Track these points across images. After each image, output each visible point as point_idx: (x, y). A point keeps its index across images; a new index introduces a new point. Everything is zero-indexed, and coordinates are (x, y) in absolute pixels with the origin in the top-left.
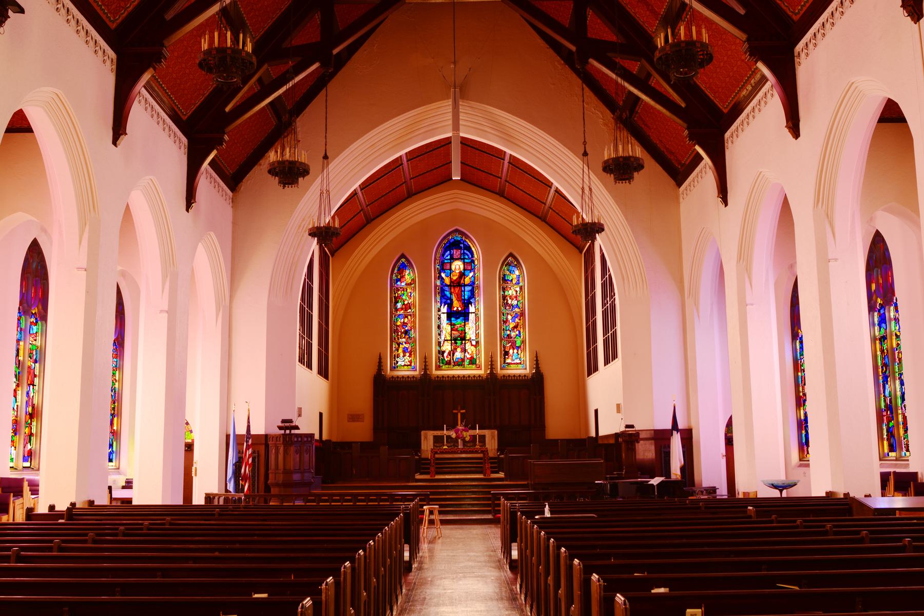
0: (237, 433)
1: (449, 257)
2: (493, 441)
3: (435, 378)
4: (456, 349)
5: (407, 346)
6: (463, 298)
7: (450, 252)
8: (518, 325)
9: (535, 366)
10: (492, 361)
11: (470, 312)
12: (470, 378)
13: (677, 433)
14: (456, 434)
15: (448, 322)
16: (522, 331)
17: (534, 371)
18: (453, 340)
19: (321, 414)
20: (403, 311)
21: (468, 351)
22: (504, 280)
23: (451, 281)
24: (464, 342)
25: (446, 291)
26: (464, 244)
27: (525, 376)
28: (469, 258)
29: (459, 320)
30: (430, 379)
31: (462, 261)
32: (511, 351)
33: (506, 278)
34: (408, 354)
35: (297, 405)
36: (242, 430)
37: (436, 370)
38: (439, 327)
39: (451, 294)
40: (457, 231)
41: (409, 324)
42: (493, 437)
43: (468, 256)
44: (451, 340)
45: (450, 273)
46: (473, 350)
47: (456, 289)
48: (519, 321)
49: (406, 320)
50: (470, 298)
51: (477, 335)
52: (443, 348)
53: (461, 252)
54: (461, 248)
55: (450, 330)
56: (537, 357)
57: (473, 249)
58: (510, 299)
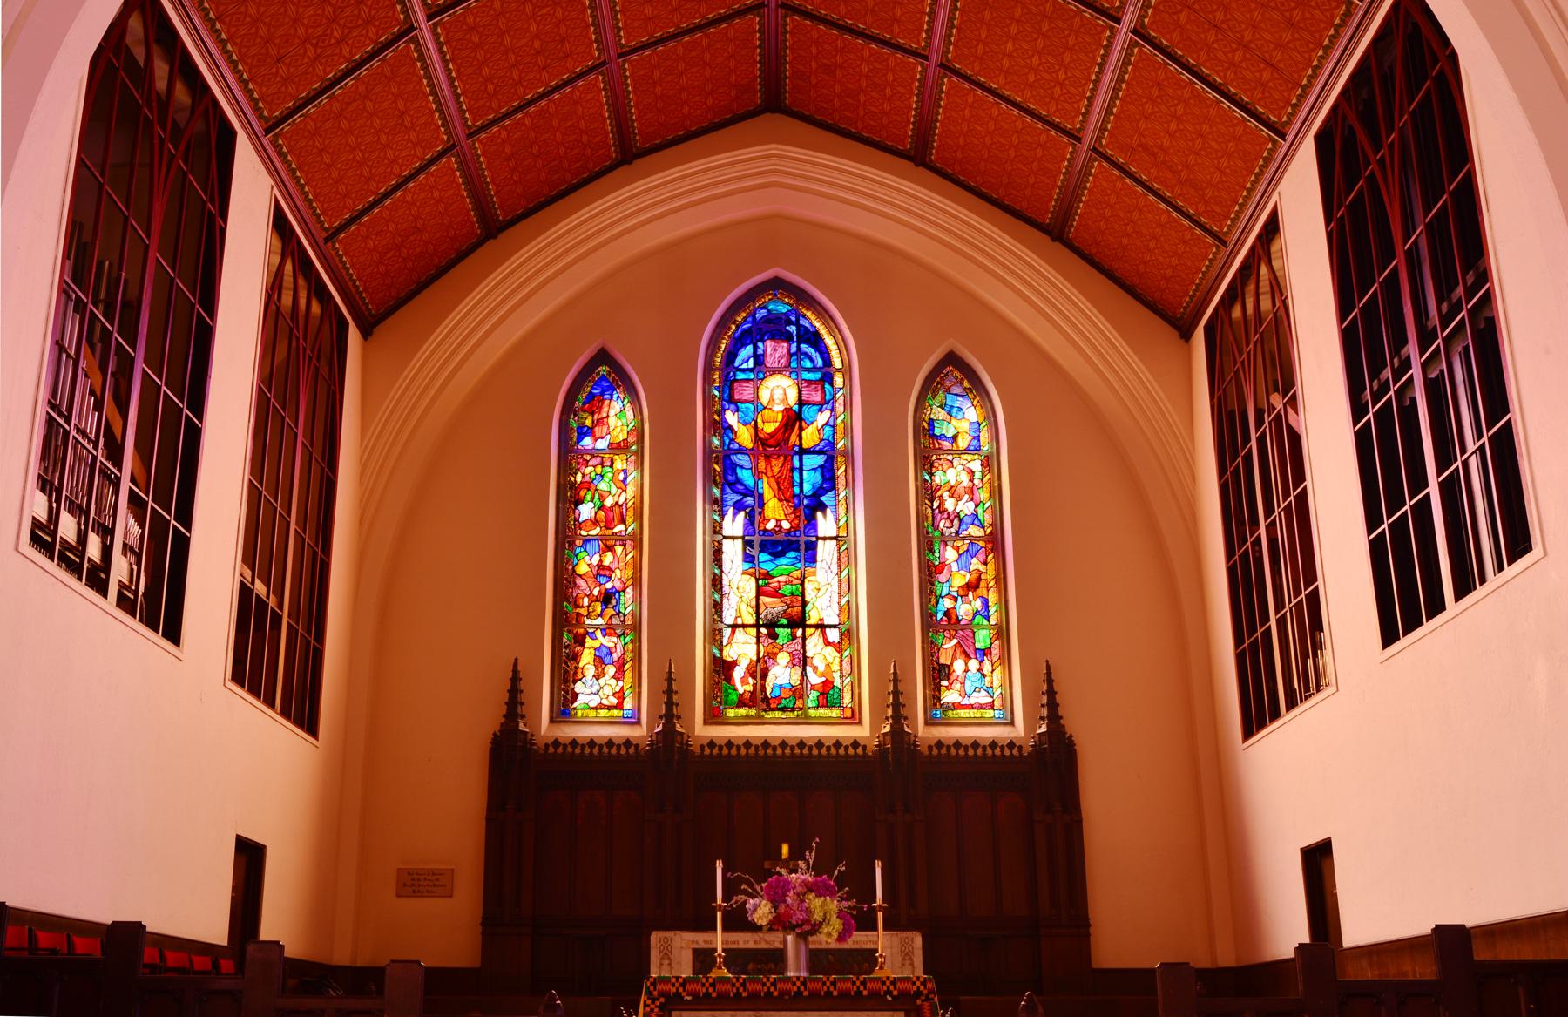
1: (751, 364)
3: (702, 747)
4: (772, 656)
5: (609, 642)
6: (797, 490)
7: (756, 348)
8: (979, 579)
9: (1045, 712)
10: (896, 693)
11: (820, 534)
12: (824, 751)
15: (747, 566)
16: (992, 598)
18: (763, 626)
20: (598, 529)
21: (815, 662)
22: (926, 433)
23: (757, 435)
24: (799, 632)
25: (742, 467)
26: (797, 324)
28: (814, 369)
29: (783, 561)
31: (794, 376)
32: (959, 666)
33: (937, 432)
34: (611, 670)
37: (705, 723)
38: (716, 583)
39: (758, 475)
40: (777, 286)
41: (618, 571)
43: (812, 360)
44: (757, 626)
45: (756, 411)
46: (830, 660)
47: (774, 462)
48: (982, 568)
49: (608, 559)
50: (819, 492)
51: (847, 610)
52: (729, 654)
53: (789, 349)
54: (788, 338)
55: (753, 593)
56: (1050, 681)
57: (829, 341)
58: (951, 496)
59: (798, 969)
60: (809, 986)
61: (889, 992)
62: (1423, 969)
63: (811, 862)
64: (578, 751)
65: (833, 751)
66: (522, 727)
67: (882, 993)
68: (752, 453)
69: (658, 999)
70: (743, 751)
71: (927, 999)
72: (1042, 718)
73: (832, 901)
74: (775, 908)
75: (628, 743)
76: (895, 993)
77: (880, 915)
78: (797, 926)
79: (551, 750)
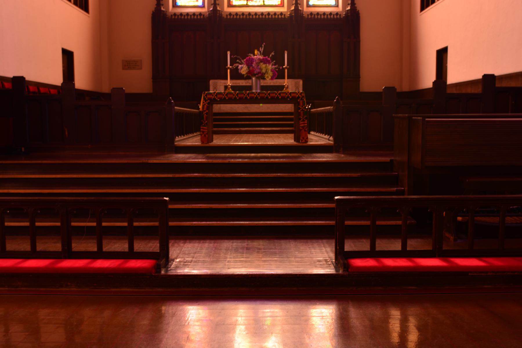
3: (227, 15)
27: (337, 14)
30: (221, 16)
59: (256, 89)
60: (260, 95)
61: (288, 97)
62: (479, 90)
63: (262, 52)
64: (183, 17)
65: (273, 17)
66: (162, 9)
67: (286, 97)
69: (207, 101)
71: (302, 99)
72: (349, 4)
73: (269, 65)
74: (249, 68)
75: (200, 14)
76: (290, 97)
77: (286, 70)
78: (257, 74)
79: (173, 17)
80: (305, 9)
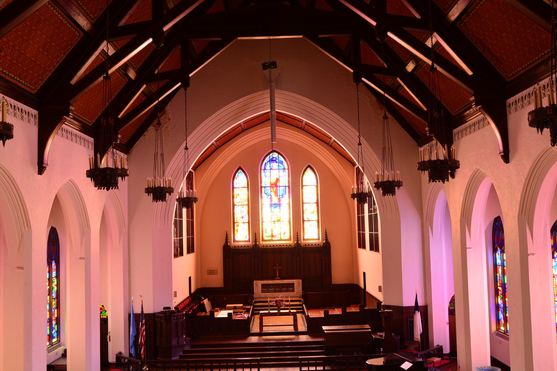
0: (134, 313)
1: (269, 168)
2: (299, 287)
8: (314, 211)
10: (297, 236)
13: (418, 312)
14: (276, 304)
17: (324, 242)
19: (190, 278)
24: (279, 222)
29: (276, 209)
30: (259, 248)
35: (174, 290)
36: (138, 311)
37: (262, 241)
42: (299, 284)
54: (277, 162)
56: (326, 232)
68: (271, 187)
70: (273, 247)
72: (324, 240)
80: (302, 242)
